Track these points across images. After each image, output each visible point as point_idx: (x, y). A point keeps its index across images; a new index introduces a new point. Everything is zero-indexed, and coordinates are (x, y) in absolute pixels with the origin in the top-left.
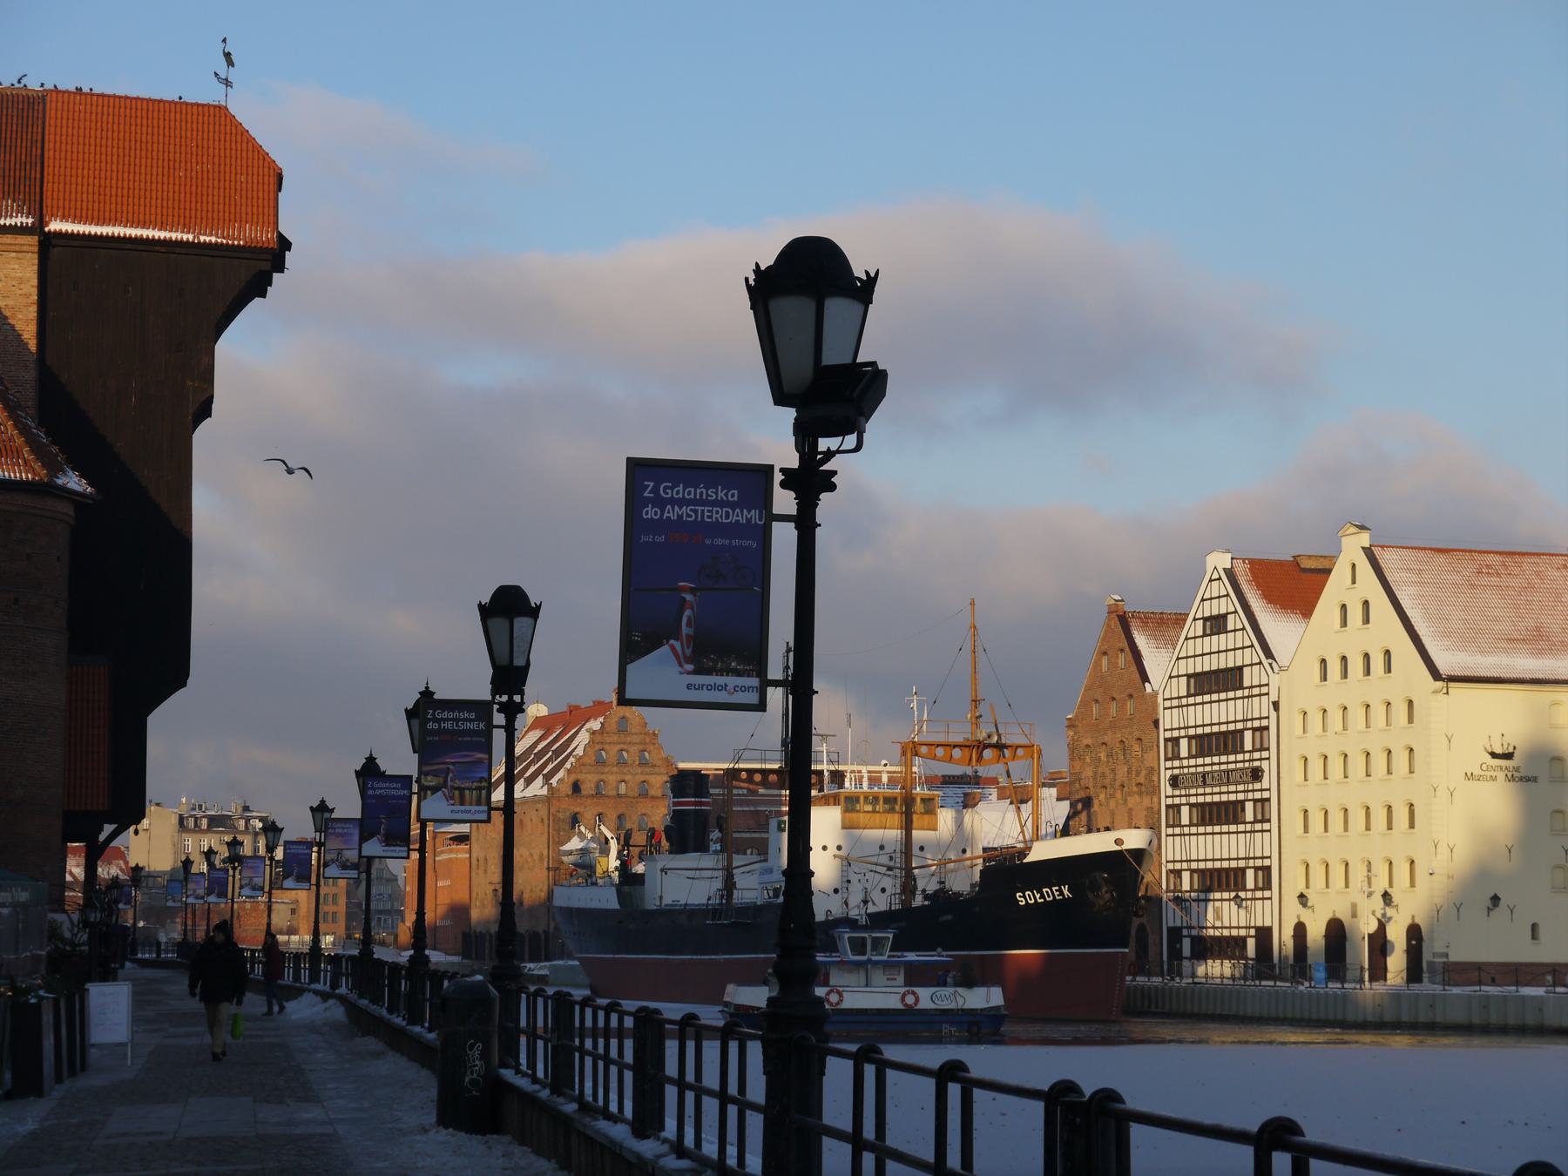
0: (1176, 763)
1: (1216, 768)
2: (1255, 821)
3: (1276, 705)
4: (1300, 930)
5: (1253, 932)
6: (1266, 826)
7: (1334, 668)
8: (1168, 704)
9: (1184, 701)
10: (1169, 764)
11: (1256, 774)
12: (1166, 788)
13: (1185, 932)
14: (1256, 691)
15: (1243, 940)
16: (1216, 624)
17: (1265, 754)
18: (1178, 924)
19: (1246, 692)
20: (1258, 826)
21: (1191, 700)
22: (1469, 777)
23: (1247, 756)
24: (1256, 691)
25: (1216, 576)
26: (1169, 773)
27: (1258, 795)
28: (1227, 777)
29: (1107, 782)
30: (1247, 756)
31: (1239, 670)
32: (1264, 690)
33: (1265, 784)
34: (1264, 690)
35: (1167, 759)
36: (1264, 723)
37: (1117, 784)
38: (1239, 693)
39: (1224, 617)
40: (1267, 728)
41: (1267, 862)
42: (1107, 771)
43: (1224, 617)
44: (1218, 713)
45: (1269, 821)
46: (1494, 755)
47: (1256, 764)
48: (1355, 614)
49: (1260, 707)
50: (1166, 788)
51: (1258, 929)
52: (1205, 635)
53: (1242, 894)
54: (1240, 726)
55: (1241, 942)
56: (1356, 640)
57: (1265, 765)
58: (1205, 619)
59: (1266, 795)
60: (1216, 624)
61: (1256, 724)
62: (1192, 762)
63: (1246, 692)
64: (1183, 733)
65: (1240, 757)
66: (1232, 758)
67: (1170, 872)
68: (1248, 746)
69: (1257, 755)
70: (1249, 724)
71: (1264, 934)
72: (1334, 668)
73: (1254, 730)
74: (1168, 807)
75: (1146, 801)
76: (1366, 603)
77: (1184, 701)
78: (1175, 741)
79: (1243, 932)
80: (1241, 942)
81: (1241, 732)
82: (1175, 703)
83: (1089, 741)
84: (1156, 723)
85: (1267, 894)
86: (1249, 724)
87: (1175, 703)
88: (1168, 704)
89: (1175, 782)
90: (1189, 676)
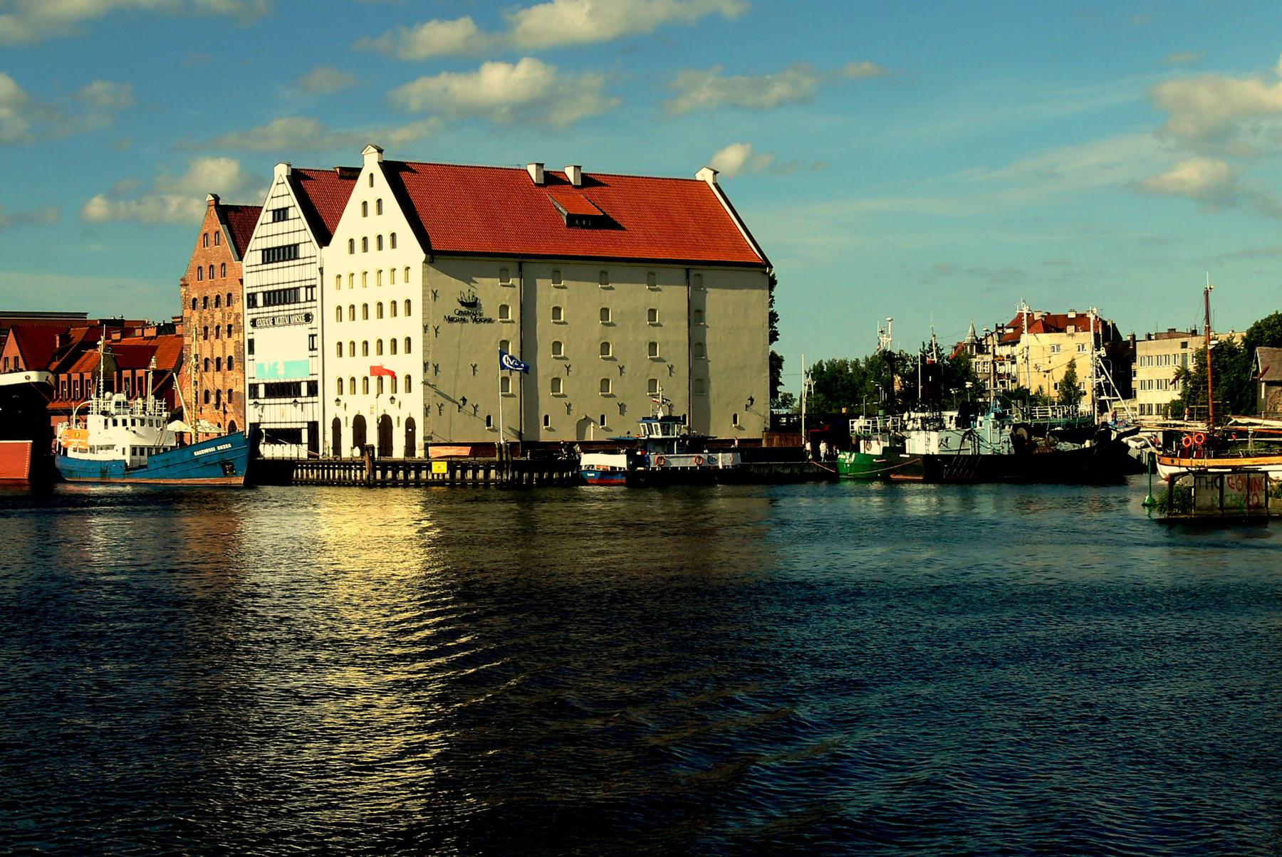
0: (255, 310)
3: (321, 270)
4: (337, 424)
5: (306, 425)
6: (314, 353)
7: (358, 245)
8: (249, 269)
9: (260, 268)
10: (250, 311)
11: (308, 318)
12: (248, 328)
14: (308, 261)
16: (280, 215)
17: (313, 304)
19: (301, 261)
21: (265, 267)
22: (451, 320)
23: (302, 305)
24: (308, 261)
26: (251, 317)
30: (302, 305)
31: (296, 246)
32: (313, 260)
33: (314, 324)
34: (313, 260)
36: (313, 283)
38: (297, 262)
41: (314, 378)
44: (281, 275)
46: (463, 304)
47: (308, 311)
48: (372, 207)
49: (311, 272)
50: (248, 328)
51: (309, 423)
52: (274, 221)
53: (299, 400)
54: (297, 285)
55: (298, 431)
56: (374, 226)
57: (313, 311)
58: (274, 211)
59: (314, 332)
60: (280, 215)
61: (308, 283)
62: (266, 309)
64: (259, 289)
65: (297, 306)
66: (292, 306)
67: (250, 385)
68: (303, 298)
69: (308, 304)
70: (303, 284)
71: (313, 427)
72: (358, 245)
73: (307, 287)
76: (379, 201)
77: (260, 268)
78: (254, 295)
79: (299, 426)
80: (298, 431)
82: (254, 269)
83: (195, 295)
84: (241, 281)
85: (315, 399)
86: (303, 284)
87: (254, 269)
88: (249, 269)
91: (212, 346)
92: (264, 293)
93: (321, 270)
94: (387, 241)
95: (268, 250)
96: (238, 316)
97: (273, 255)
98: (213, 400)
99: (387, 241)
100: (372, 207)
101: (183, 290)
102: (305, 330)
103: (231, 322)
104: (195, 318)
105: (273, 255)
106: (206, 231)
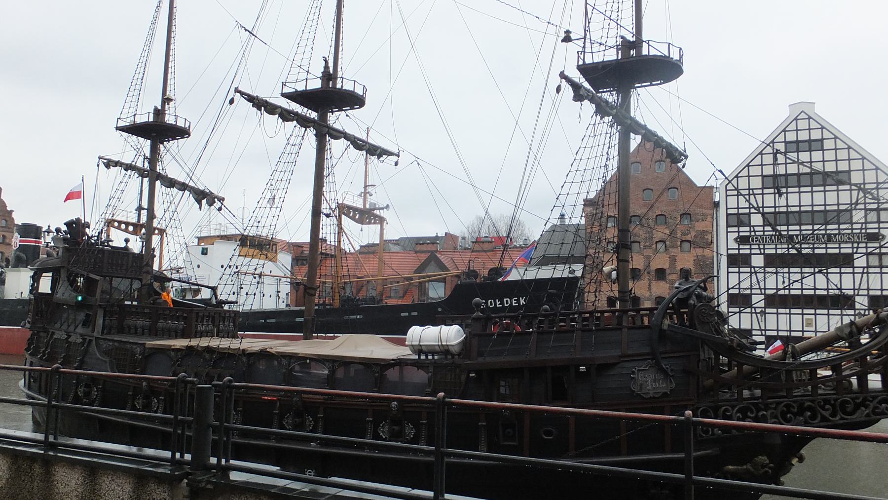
2: (868, 267)
10: (736, 229)
13: (754, 332)
18: (746, 326)
20: (871, 270)
23: (859, 226)
25: (803, 116)
26: (733, 236)
28: (830, 238)
35: (728, 226)
37: (655, 240)
39: (821, 140)
43: (821, 140)
47: (868, 231)
58: (786, 143)
69: (869, 226)
73: (866, 210)
74: (729, 256)
75: (699, 251)
84: (717, 205)
89: (742, 240)
90: (763, 176)
95: (775, 176)
96: (704, 233)
101: (588, 209)
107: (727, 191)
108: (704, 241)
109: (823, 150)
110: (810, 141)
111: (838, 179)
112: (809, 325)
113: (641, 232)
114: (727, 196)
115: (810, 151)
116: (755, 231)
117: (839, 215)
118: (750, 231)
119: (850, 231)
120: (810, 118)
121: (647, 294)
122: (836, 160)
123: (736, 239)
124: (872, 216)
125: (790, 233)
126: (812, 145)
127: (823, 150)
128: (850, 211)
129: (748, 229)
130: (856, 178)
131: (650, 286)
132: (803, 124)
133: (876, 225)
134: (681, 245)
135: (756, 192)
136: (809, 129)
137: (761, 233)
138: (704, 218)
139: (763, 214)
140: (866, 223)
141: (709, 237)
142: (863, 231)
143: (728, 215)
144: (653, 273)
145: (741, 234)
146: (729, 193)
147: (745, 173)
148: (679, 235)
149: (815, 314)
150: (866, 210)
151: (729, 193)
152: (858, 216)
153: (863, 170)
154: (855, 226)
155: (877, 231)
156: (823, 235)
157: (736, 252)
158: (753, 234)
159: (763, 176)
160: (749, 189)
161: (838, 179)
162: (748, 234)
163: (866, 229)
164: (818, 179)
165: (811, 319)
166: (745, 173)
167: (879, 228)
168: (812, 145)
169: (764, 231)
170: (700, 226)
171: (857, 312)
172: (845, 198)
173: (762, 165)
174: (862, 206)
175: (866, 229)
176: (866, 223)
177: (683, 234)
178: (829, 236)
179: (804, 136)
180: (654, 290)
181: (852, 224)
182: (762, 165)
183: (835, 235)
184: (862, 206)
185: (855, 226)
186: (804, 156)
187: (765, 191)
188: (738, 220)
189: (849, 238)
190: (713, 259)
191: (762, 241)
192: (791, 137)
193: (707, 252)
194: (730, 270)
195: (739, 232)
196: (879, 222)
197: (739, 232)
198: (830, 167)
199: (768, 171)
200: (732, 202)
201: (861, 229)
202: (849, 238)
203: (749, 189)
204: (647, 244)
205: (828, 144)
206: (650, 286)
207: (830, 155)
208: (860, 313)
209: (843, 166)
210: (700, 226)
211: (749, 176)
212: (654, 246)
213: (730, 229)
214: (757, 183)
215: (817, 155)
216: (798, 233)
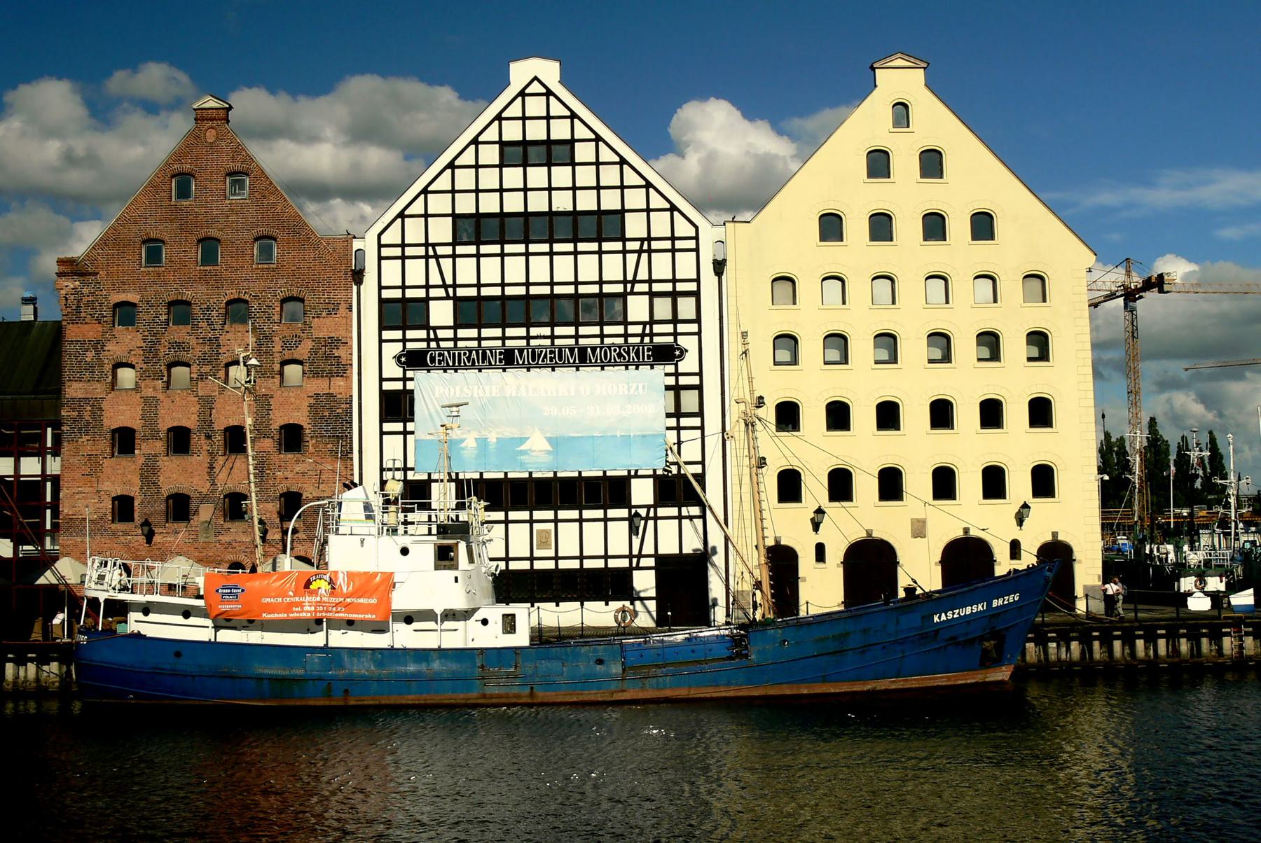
1: (548, 342)
3: (719, 267)
5: (651, 562)
7: (856, 228)
10: (398, 334)
15: (626, 574)
17: (681, 328)
23: (638, 329)
25: (536, 88)
27: (671, 381)
29: (184, 356)
32: (692, 244)
35: (382, 328)
37: (224, 359)
39: (572, 142)
40: (696, 294)
42: (193, 341)
43: (572, 142)
45: (700, 414)
47: (656, 339)
48: (905, 163)
51: (656, 556)
58: (502, 144)
59: (683, 381)
61: (668, 287)
63: (635, 246)
65: (619, 329)
69: (657, 328)
72: (856, 228)
73: (652, 295)
74: (385, 396)
75: (320, 386)
80: (626, 574)
81: (623, 296)
82: (421, 251)
83: (133, 297)
87: (421, 251)
90: (455, 216)
91: (208, 403)
92: (457, 300)
93: (719, 267)
94: (959, 227)
95: (478, 216)
97: (476, 230)
98: (205, 513)
99: (959, 227)
100: (905, 163)
101: (71, 283)
102: (659, 375)
103: (303, 351)
104: (126, 342)
105: (476, 230)
106: (186, 167)
107: (380, 246)
108: (331, 361)
109: (573, 164)
110: (549, 143)
111: (603, 227)
112: (544, 545)
113: (193, 341)
114: (380, 258)
115: (549, 164)
116: (437, 340)
117: (604, 306)
118: (428, 340)
119: (621, 341)
120: (549, 93)
121: (205, 488)
122: (598, 188)
123: (398, 358)
124: (663, 308)
125: (509, 343)
126: (555, 153)
127: (573, 164)
128: (623, 296)
129: (422, 334)
130: (635, 226)
131: (211, 468)
132: (536, 106)
133: (669, 328)
134: (281, 373)
135: (441, 251)
136: (548, 118)
137: (451, 344)
138: (332, 310)
139: (457, 300)
140: (652, 322)
141: (341, 352)
142: (647, 340)
143: (382, 302)
144: (219, 438)
145: (410, 345)
146: (385, 252)
147: (418, 208)
148: (278, 348)
149: (556, 521)
150: (652, 295)
151: (385, 252)
152: (637, 308)
153: (648, 210)
154: (632, 329)
155: (670, 339)
156: (572, 350)
157: (398, 386)
158: (433, 345)
159: (455, 216)
160: (426, 245)
161: (603, 227)
162: (424, 345)
163: (652, 335)
164: (563, 227)
165: (548, 532)
166: (418, 208)
167: (675, 334)
168: (555, 153)
169: (455, 339)
170: (324, 327)
171: (633, 511)
172: (613, 267)
173: (453, 191)
174: (644, 287)
175: (652, 335)
176: (652, 322)
177: (287, 345)
178: (583, 350)
179: (536, 131)
180: (222, 477)
181: (625, 323)
182: (453, 191)
183: (594, 349)
184: (645, 287)
185: (632, 329)
186: (537, 175)
187: (460, 250)
188: (402, 313)
189: (620, 355)
190: (351, 403)
191: (455, 361)
192: (512, 132)
193: (339, 383)
194: (388, 427)
195: (404, 340)
196: (675, 321)
197: (404, 340)
198: (587, 202)
199: (465, 205)
200: (391, 274)
201: (643, 335)
202: (620, 355)
203: (426, 245)
204: (207, 369)
205: (584, 152)
206: (211, 468)
207: (586, 176)
208: (637, 515)
209: (611, 201)
210: (324, 327)
211: (426, 216)
212: (222, 374)
213: (387, 335)
214: (442, 231)
215: (562, 175)
216: (523, 343)
